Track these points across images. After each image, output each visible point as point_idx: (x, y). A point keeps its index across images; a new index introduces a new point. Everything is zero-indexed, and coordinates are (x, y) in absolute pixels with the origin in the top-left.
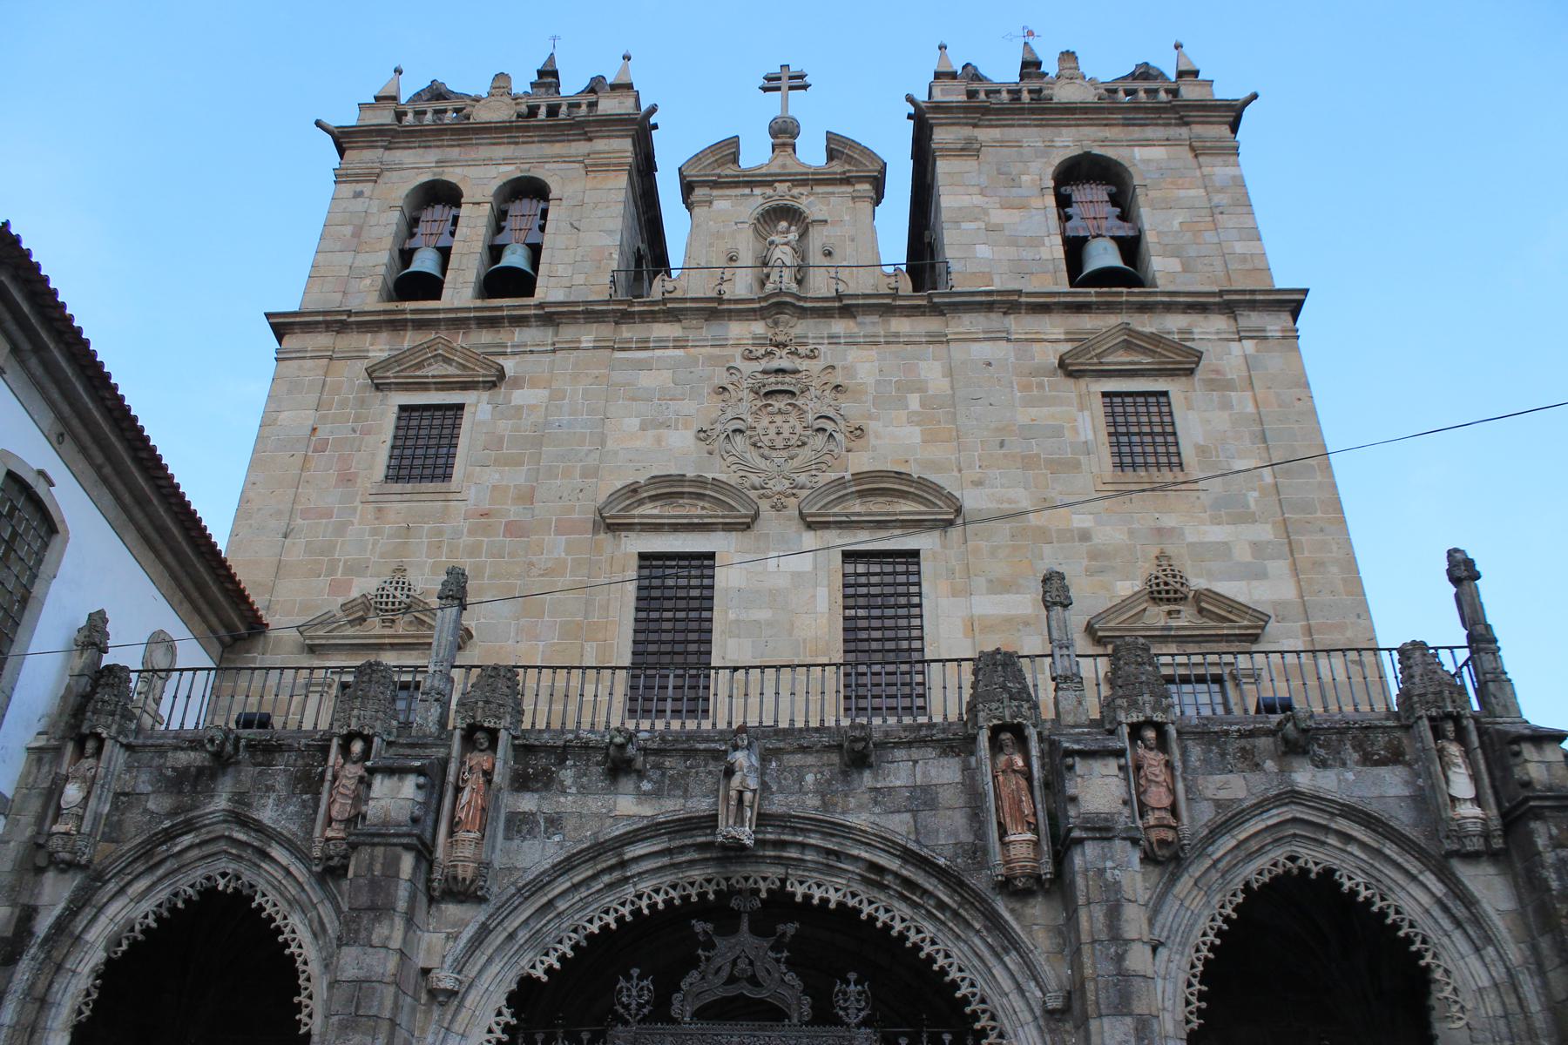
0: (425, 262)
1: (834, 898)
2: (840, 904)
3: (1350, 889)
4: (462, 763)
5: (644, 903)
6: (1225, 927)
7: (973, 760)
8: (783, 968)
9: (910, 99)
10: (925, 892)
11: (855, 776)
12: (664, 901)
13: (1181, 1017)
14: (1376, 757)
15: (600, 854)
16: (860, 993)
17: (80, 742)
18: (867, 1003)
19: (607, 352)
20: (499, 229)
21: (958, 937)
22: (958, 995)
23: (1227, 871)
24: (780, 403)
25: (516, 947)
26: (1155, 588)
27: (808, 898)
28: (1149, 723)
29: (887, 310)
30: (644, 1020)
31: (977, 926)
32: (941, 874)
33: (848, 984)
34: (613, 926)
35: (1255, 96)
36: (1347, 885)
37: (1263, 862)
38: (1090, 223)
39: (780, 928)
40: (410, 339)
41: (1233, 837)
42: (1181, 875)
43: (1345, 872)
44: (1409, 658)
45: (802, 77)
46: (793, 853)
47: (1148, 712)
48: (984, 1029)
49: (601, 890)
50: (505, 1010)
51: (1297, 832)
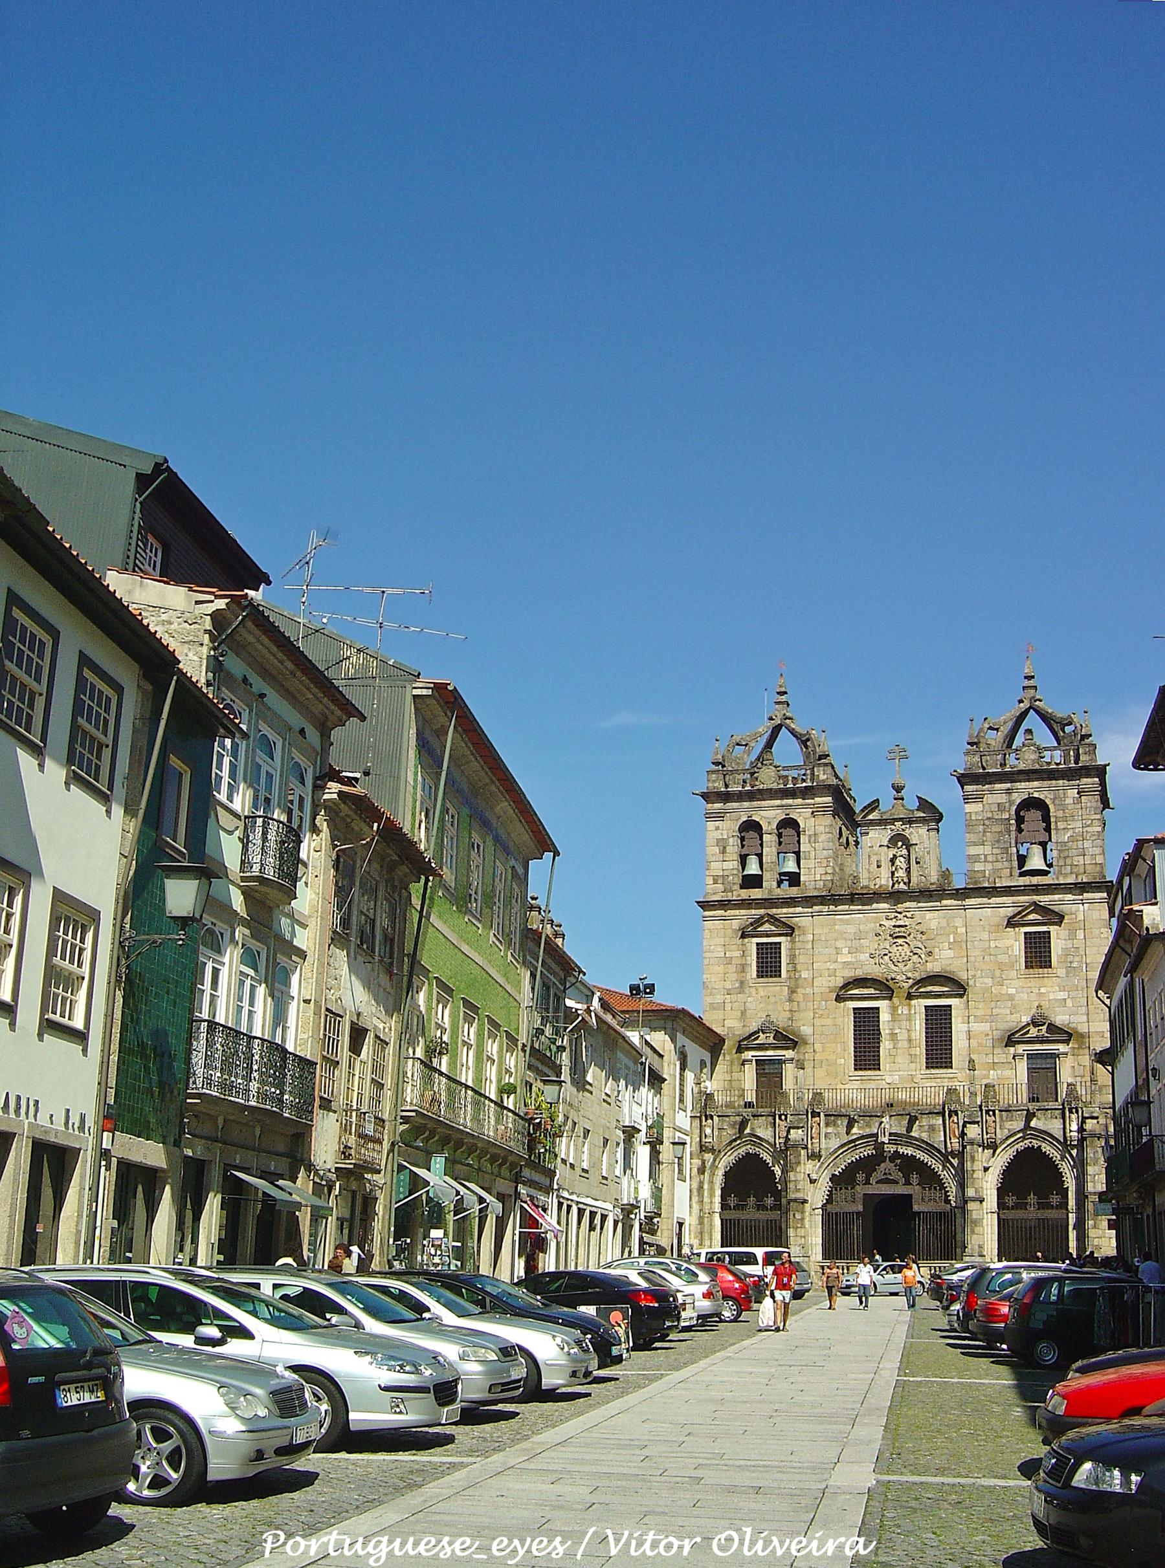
1: (910, 1153)
17: (706, 1116)
35: (1108, 765)
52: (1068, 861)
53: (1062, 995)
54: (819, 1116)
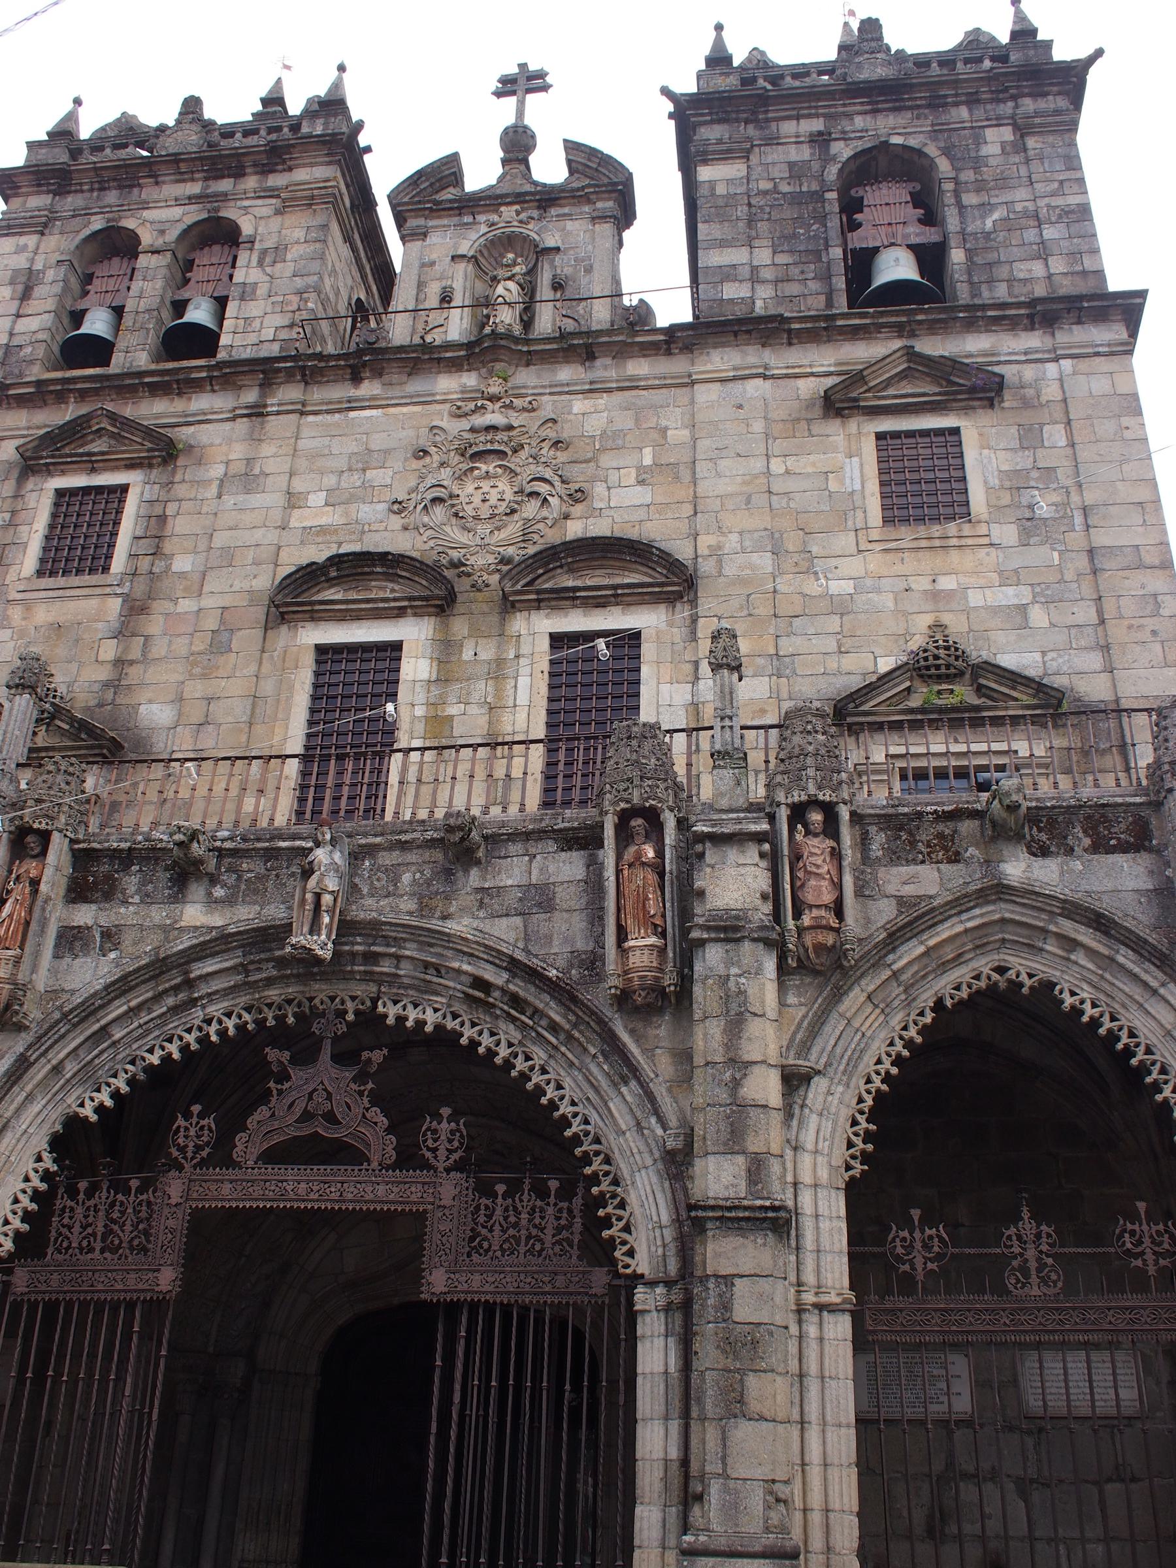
0: (97, 324)
1: (431, 1018)
2: (438, 1027)
3: (1073, 1007)
4: (10, 872)
5: (213, 1029)
6: (906, 1053)
7: (601, 852)
8: (366, 1100)
9: (666, 92)
10: (536, 1011)
11: (460, 874)
12: (237, 1027)
13: (838, 1161)
14: (1113, 842)
15: (162, 973)
16: (452, 1132)
18: (462, 1144)
19: (294, 417)
20: (187, 281)
21: (572, 1064)
22: (568, 1133)
23: (912, 985)
24: (487, 466)
25: (62, 1082)
26: (922, 663)
27: (401, 1019)
28: (813, 803)
29: (622, 353)
30: (203, 1163)
31: (593, 1051)
32: (554, 988)
33: (439, 1123)
34: (176, 1056)
35: (1099, 53)
36: (1069, 1001)
37: (962, 973)
38: (883, 230)
39: (365, 1055)
40: (70, 412)
41: (922, 943)
42: (850, 989)
43: (1066, 986)
44: (1165, 718)
45: (541, 75)
46: (386, 967)
47: (812, 789)
48: (595, 1174)
49: (164, 1014)
50: (45, 1155)
51: (1007, 936)
52: (1003, 272)
53: (1010, 595)
54: (44, 853)
